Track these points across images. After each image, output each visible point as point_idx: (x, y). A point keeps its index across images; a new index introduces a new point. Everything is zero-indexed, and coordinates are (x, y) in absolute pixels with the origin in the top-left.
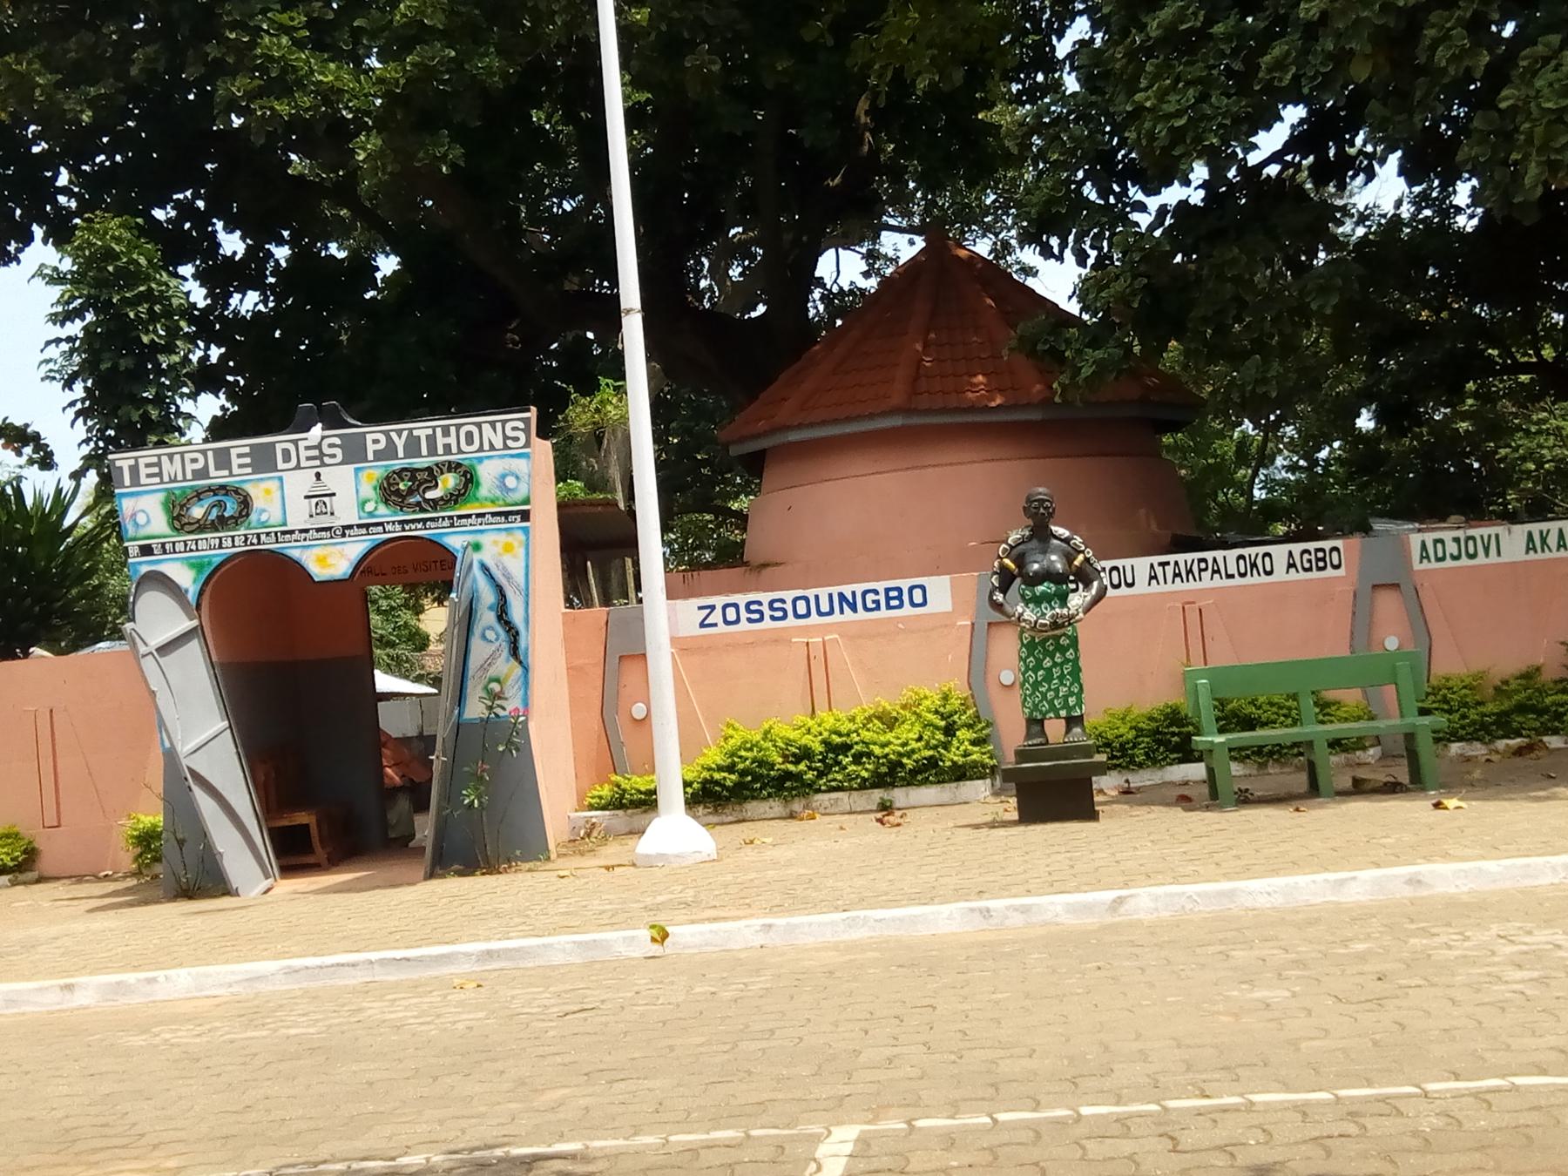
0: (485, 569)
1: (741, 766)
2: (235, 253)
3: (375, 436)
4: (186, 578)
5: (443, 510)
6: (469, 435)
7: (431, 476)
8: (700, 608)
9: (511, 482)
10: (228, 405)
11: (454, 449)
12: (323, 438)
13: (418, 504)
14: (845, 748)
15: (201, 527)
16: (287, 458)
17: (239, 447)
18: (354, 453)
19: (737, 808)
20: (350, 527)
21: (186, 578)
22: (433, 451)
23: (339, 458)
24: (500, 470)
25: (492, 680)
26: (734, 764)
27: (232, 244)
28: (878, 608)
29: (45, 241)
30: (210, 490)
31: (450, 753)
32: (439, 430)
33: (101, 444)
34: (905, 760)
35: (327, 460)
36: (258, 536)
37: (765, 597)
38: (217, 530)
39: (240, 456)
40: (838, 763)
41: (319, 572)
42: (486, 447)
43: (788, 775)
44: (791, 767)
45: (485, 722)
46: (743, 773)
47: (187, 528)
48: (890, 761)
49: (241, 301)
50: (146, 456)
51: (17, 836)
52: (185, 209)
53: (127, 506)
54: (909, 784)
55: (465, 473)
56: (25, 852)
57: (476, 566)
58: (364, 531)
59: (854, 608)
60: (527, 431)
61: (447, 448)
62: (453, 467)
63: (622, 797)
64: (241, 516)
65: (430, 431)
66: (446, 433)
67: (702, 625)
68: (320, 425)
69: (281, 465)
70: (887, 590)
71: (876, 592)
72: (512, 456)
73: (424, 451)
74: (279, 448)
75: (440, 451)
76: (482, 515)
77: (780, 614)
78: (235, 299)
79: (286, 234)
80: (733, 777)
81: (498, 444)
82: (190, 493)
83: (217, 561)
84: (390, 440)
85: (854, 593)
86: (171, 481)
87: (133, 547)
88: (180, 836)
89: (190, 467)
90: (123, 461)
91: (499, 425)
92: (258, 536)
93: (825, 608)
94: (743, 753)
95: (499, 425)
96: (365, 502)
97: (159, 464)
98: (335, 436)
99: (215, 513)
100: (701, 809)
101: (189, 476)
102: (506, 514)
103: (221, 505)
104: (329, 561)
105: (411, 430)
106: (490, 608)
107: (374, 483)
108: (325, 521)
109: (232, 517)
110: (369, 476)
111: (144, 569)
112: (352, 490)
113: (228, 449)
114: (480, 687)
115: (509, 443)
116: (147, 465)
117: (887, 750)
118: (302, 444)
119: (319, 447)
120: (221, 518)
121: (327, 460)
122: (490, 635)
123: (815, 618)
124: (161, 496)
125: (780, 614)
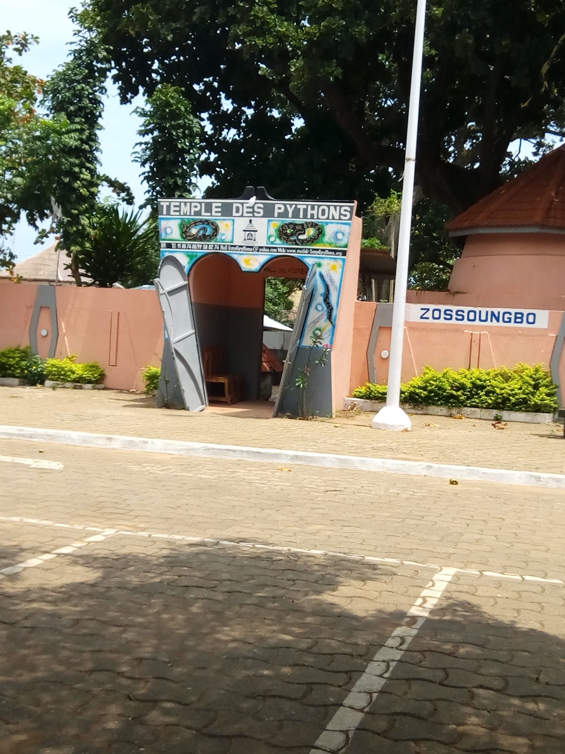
0: (321, 276)
1: (430, 388)
2: (228, 110)
3: (279, 206)
4: (185, 261)
5: (306, 245)
6: (323, 211)
7: (302, 228)
8: (422, 309)
9: (340, 236)
10: (215, 182)
11: (315, 217)
12: (256, 203)
13: (295, 241)
14: (482, 387)
16: (237, 211)
17: (217, 203)
18: (269, 213)
19: (425, 408)
20: (262, 247)
21: (185, 261)
22: (305, 216)
23: (261, 214)
24: (336, 230)
26: (427, 387)
27: (227, 105)
28: (510, 322)
29: (144, 95)
30: (201, 221)
31: (293, 360)
32: (309, 207)
33: (155, 194)
34: (511, 398)
35: (256, 214)
36: (220, 246)
37: (455, 308)
38: (201, 241)
39: (217, 207)
40: (478, 394)
42: (331, 217)
43: (452, 396)
44: (454, 392)
45: (311, 348)
46: (430, 392)
47: (188, 238)
48: (504, 397)
49: (228, 133)
50: (175, 202)
51: (97, 367)
52: (208, 86)
53: (163, 224)
54: (511, 410)
55: (319, 229)
56: (100, 375)
57: (317, 276)
58: (268, 250)
59: (498, 320)
60: (351, 212)
61: (312, 215)
62: (314, 225)
63: (370, 394)
65: (305, 207)
66: (313, 209)
67: (422, 317)
68: (255, 197)
69: (234, 214)
70: (516, 313)
71: (510, 314)
73: (301, 216)
75: (309, 216)
76: (324, 250)
77: (460, 317)
78: (224, 133)
79: (253, 103)
80: (425, 393)
81: (337, 217)
83: (199, 255)
84: (286, 208)
85: (499, 313)
86: (184, 215)
87: (163, 243)
88: (167, 379)
89: (193, 209)
90: (164, 203)
91: (338, 208)
92: (220, 246)
93: (483, 318)
94: (432, 382)
95: (338, 208)
96: (269, 237)
97: (180, 206)
98: (261, 204)
99: (201, 233)
100: (407, 405)
101: (192, 214)
102: (335, 251)
103: (205, 229)
104: (251, 262)
105: (296, 205)
106: (321, 295)
107: (276, 228)
108: (250, 243)
109: (209, 236)
110: (274, 225)
111: (167, 254)
112: (265, 230)
113: (211, 203)
114: (311, 332)
115: (342, 217)
116: (175, 206)
117: (503, 391)
118: (245, 205)
121: (256, 214)
122: (320, 308)
123: (477, 322)
124: (178, 222)
125: (460, 317)
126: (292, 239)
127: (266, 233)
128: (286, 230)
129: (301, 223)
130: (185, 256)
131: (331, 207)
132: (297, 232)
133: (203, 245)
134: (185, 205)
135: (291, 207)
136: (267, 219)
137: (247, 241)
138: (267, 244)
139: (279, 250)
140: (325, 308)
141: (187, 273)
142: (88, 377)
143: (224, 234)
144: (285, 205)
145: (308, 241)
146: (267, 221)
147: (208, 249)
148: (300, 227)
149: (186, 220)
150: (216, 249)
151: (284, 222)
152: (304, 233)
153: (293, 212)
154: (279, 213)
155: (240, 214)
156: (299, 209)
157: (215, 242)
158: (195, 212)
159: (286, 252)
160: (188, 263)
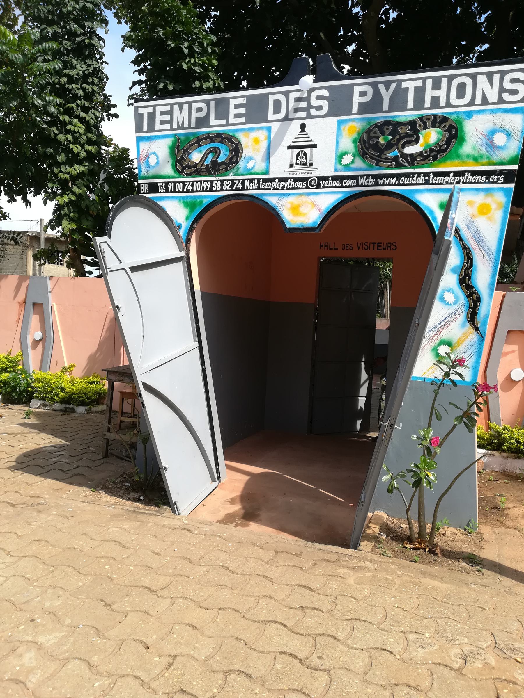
5: (420, 166)
6: (462, 87)
7: (413, 130)
9: (500, 139)
13: (395, 159)
15: (198, 170)
16: (277, 110)
18: (339, 106)
20: (325, 179)
22: (419, 104)
24: (490, 126)
25: (443, 343)
32: (429, 83)
35: (313, 112)
36: (243, 181)
38: (210, 175)
39: (237, 106)
41: (291, 219)
42: (478, 100)
45: (437, 386)
47: (187, 171)
50: (163, 105)
58: (338, 183)
61: (435, 101)
62: (438, 121)
64: (231, 163)
65: (419, 83)
66: (437, 85)
69: (271, 116)
72: (506, 111)
73: (410, 105)
74: (272, 99)
75: (427, 104)
76: (461, 174)
81: (493, 97)
82: (193, 140)
83: (206, 201)
84: (377, 93)
86: (179, 128)
89: (195, 115)
91: (496, 77)
92: (243, 181)
95: (496, 77)
97: (170, 113)
101: (193, 124)
102: (488, 174)
103: (216, 151)
104: (302, 210)
105: (400, 82)
106: (454, 271)
107: (355, 135)
109: (223, 163)
112: (332, 142)
115: (506, 97)
116: (162, 113)
119: (308, 99)
120: (214, 163)
121: (313, 112)
122: (449, 297)
124: (169, 141)
126: (390, 155)
127: (335, 149)
128: (378, 138)
129: (409, 119)
130: (182, 205)
131: (479, 77)
132: (399, 140)
133: (212, 182)
134: (181, 109)
135: (387, 89)
136: (335, 119)
137: (296, 168)
138: (336, 171)
139: (362, 181)
140: (462, 298)
141: (184, 240)
142: (80, 397)
143: (251, 159)
144: (374, 86)
145: (426, 158)
146: (336, 125)
147: (222, 190)
148: (406, 130)
149: (182, 138)
150: (237, 189)
151: (373, 122)
152: (417, 141)
153: (391, 99)
154: (360, 104)
155: (282, 115)
156: (407, 89)
157: (235, 175)
158: (198, 120)
159: (377, 184)
160: (187, 218)
